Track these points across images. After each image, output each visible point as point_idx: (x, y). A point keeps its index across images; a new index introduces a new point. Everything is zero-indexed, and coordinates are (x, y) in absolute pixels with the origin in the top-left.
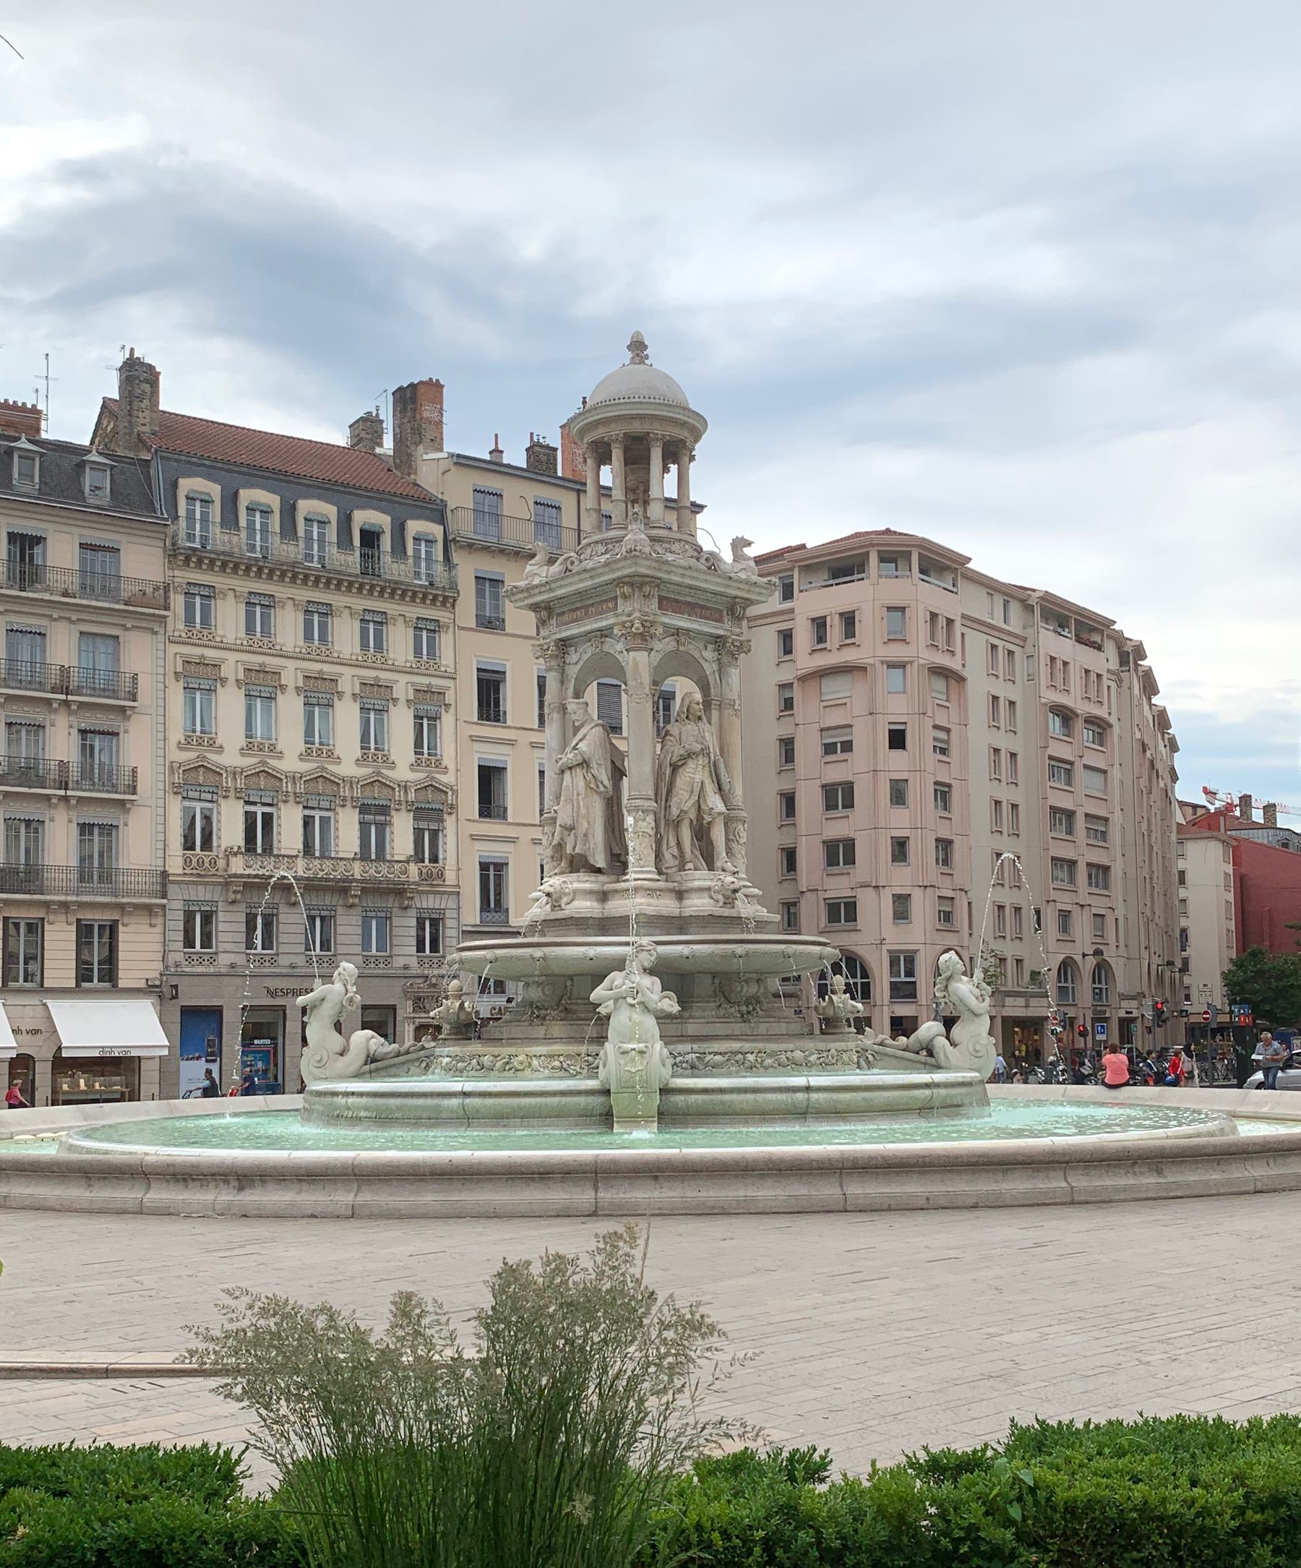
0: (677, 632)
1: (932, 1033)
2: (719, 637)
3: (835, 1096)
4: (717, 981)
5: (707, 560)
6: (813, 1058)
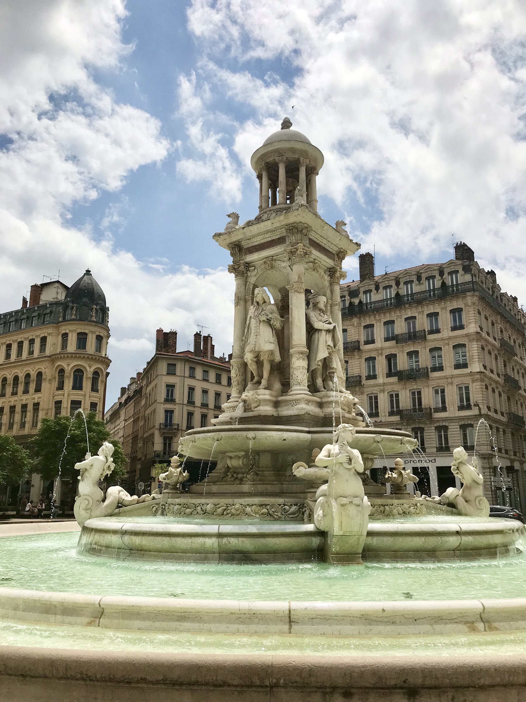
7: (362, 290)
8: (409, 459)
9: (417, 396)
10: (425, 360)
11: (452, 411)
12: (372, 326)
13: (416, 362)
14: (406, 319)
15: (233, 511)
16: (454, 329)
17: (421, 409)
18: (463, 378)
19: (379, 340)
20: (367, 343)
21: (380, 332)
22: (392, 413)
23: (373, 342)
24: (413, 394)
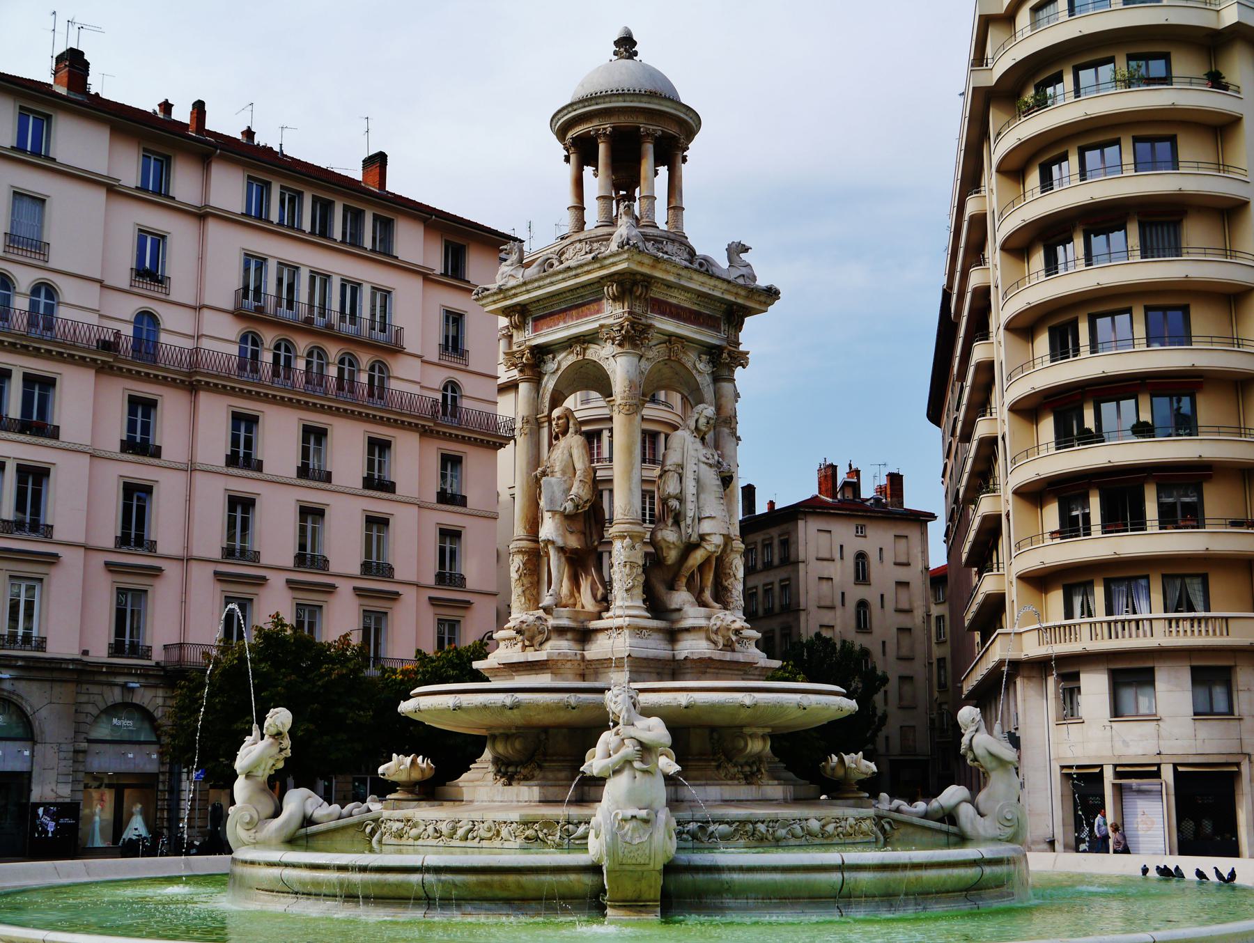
0: (671, 338)
1: (953, 802)
2: (720, 349)
4: (715, 736)
5: (701, 265)
6: (830, 828)
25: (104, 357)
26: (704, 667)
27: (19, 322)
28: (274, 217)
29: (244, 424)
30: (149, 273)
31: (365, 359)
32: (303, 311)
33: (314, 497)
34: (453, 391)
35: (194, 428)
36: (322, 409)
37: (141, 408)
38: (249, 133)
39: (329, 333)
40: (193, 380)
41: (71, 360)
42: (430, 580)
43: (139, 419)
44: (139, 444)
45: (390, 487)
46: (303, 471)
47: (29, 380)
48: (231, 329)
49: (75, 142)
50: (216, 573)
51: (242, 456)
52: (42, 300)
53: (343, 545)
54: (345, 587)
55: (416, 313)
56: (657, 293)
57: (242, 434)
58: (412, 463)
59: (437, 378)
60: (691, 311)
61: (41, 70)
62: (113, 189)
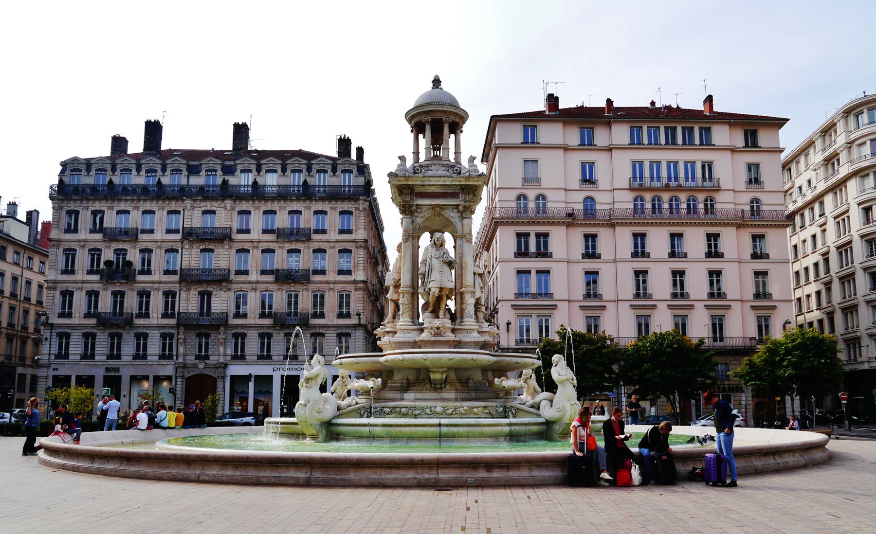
0: (433, 207)
3: (451, 429)
7: (239, 168)
8: (278, 367)
9: (293, 300)
10: (304, 261)
11: (331, 318)
12: (249, 212)
13: (296, 261)
14: (290, 212)
15: (463, 411)
16: (341, 232)
17: (296, 313)
18: (345, 285)
19: (256, 231)
20: (240, 231)
21: (257, 221)
22: (262, 315)
23: (247, 231)
24: (290, 296)
25: (570, 220)
26: (426, 343)
27: (531, 213)
28: (646, 141)
29: (639, 238)
30: (588, 179)
31: (701, 197)
32: (665, 181)
33: (678, 265)
34: (757, 202)
35: (616, 244)
36: (678, 224)
37: (590, 238)
38: (653, 103)
39: (680, 188)
40: (612, 223)
41: (553, 224)
42: (751, 297)
43: (590, 243)
44: (591, 254)
45: (721, 256)
46: (673, 254)
47: (538, 235)
48: (630, 196)
49: (549, 133)
50: (631, 306)
51: (639, 252)
52: (541, 201)
53: (697, 285)
54: (700, 306)
55: (729, 171)
56: (417, 190)
57: (639, 242)
58: (735, 243)
59: (746, 198)
60: (440, 193)
61: (541, 106)
62: (566, 149)
